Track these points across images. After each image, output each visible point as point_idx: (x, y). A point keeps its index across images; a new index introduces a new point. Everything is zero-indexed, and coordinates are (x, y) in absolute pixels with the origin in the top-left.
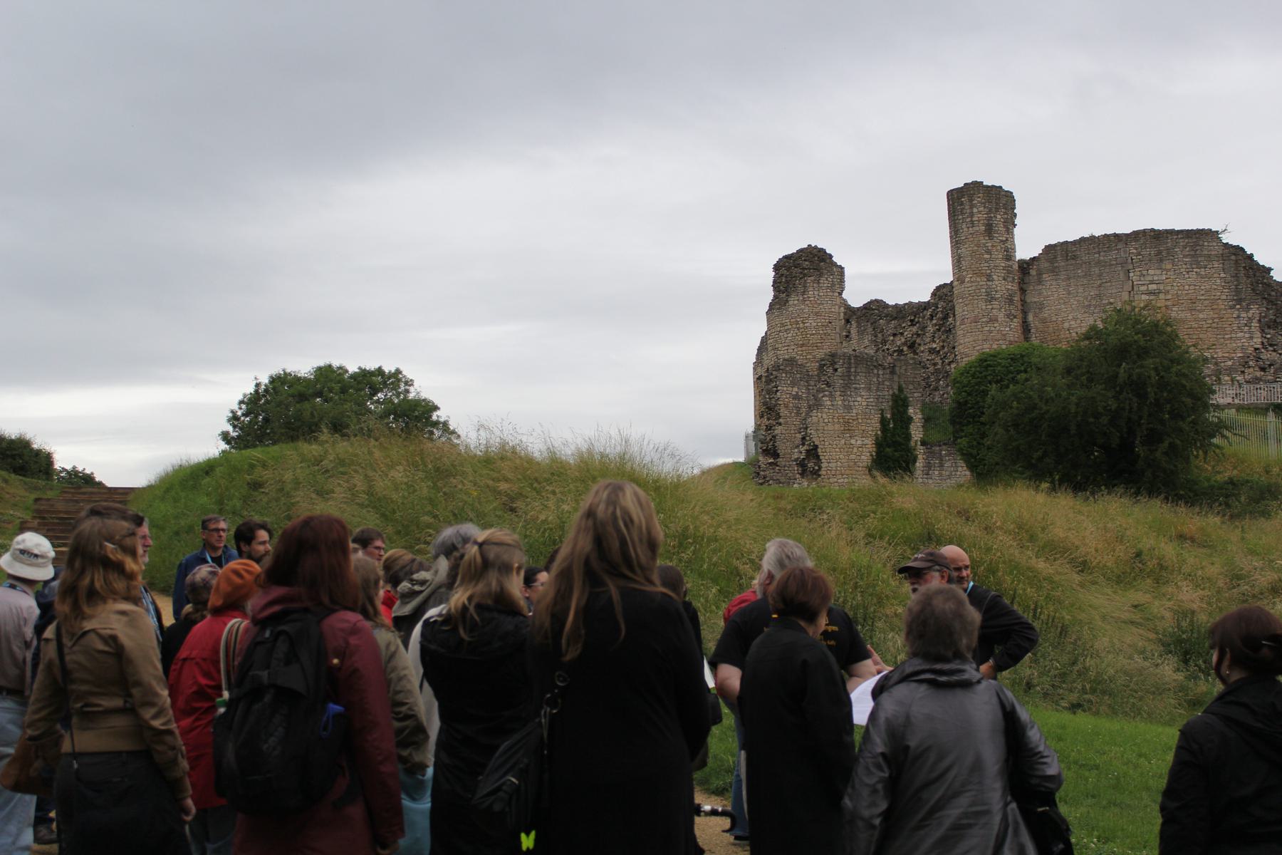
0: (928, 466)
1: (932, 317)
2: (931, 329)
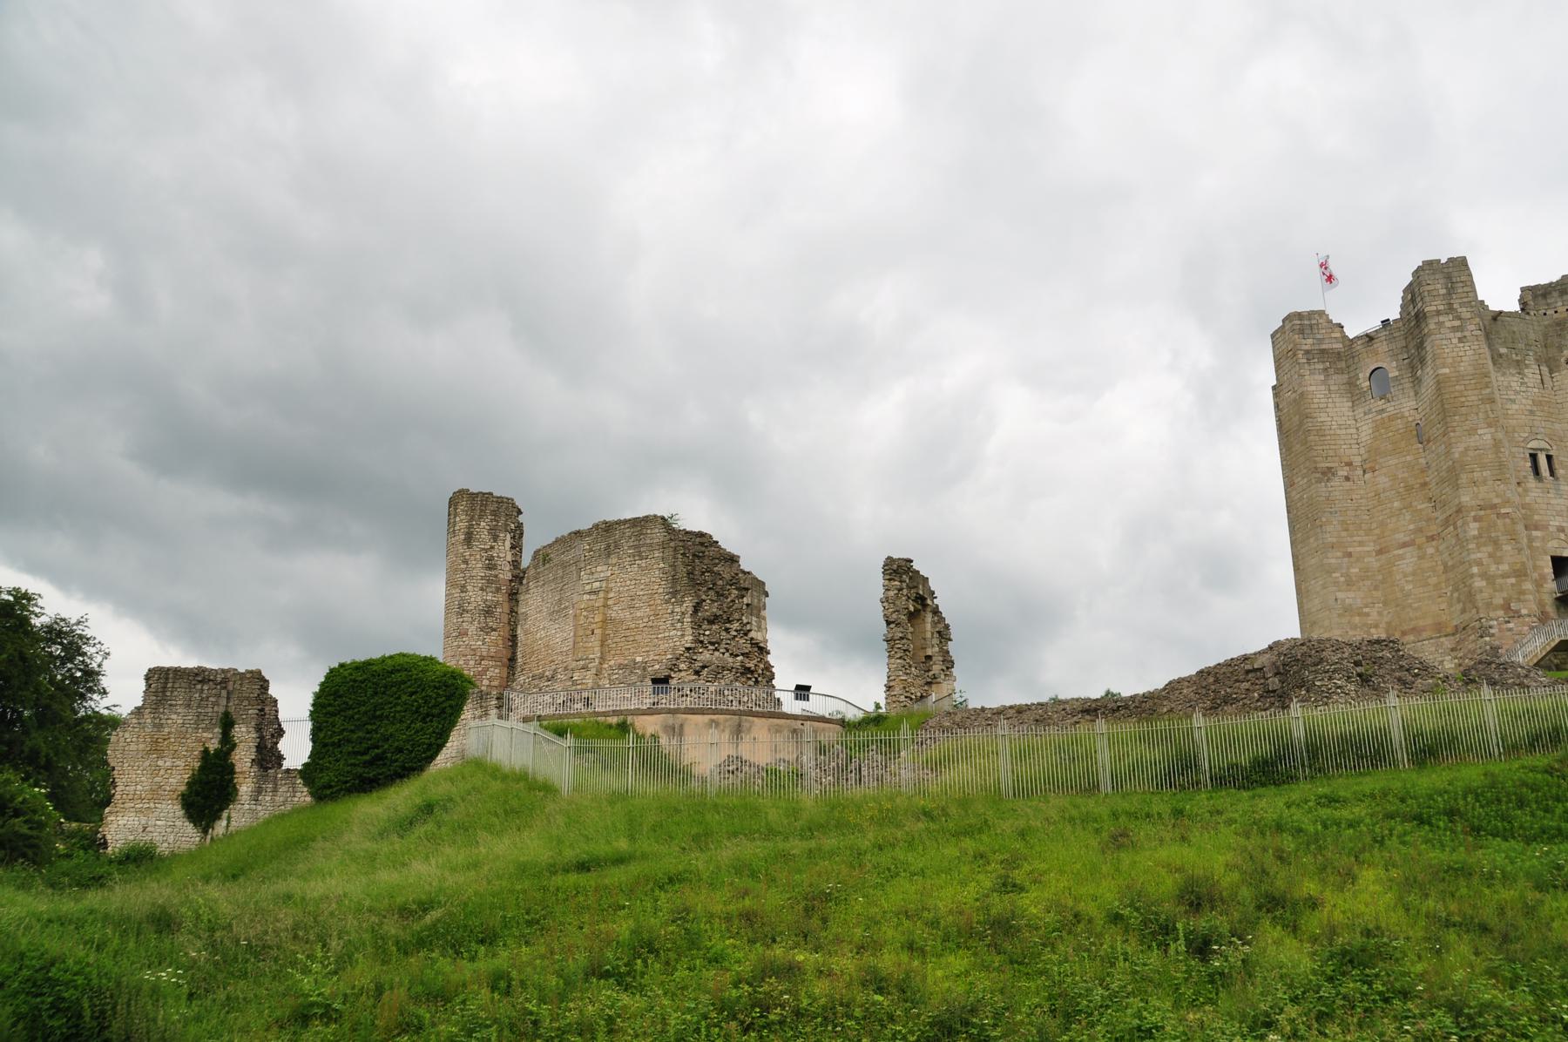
0: (259, 791)
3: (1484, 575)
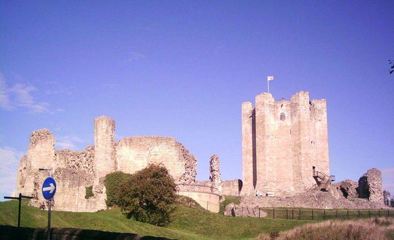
1: (85, 156)
2: (85, 159)
3: (304, 170)
